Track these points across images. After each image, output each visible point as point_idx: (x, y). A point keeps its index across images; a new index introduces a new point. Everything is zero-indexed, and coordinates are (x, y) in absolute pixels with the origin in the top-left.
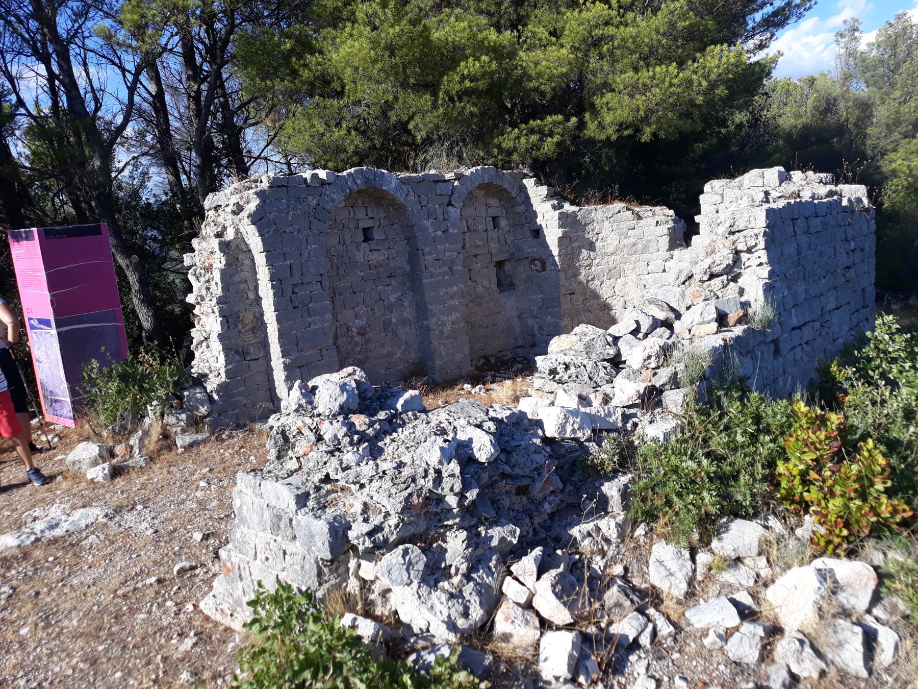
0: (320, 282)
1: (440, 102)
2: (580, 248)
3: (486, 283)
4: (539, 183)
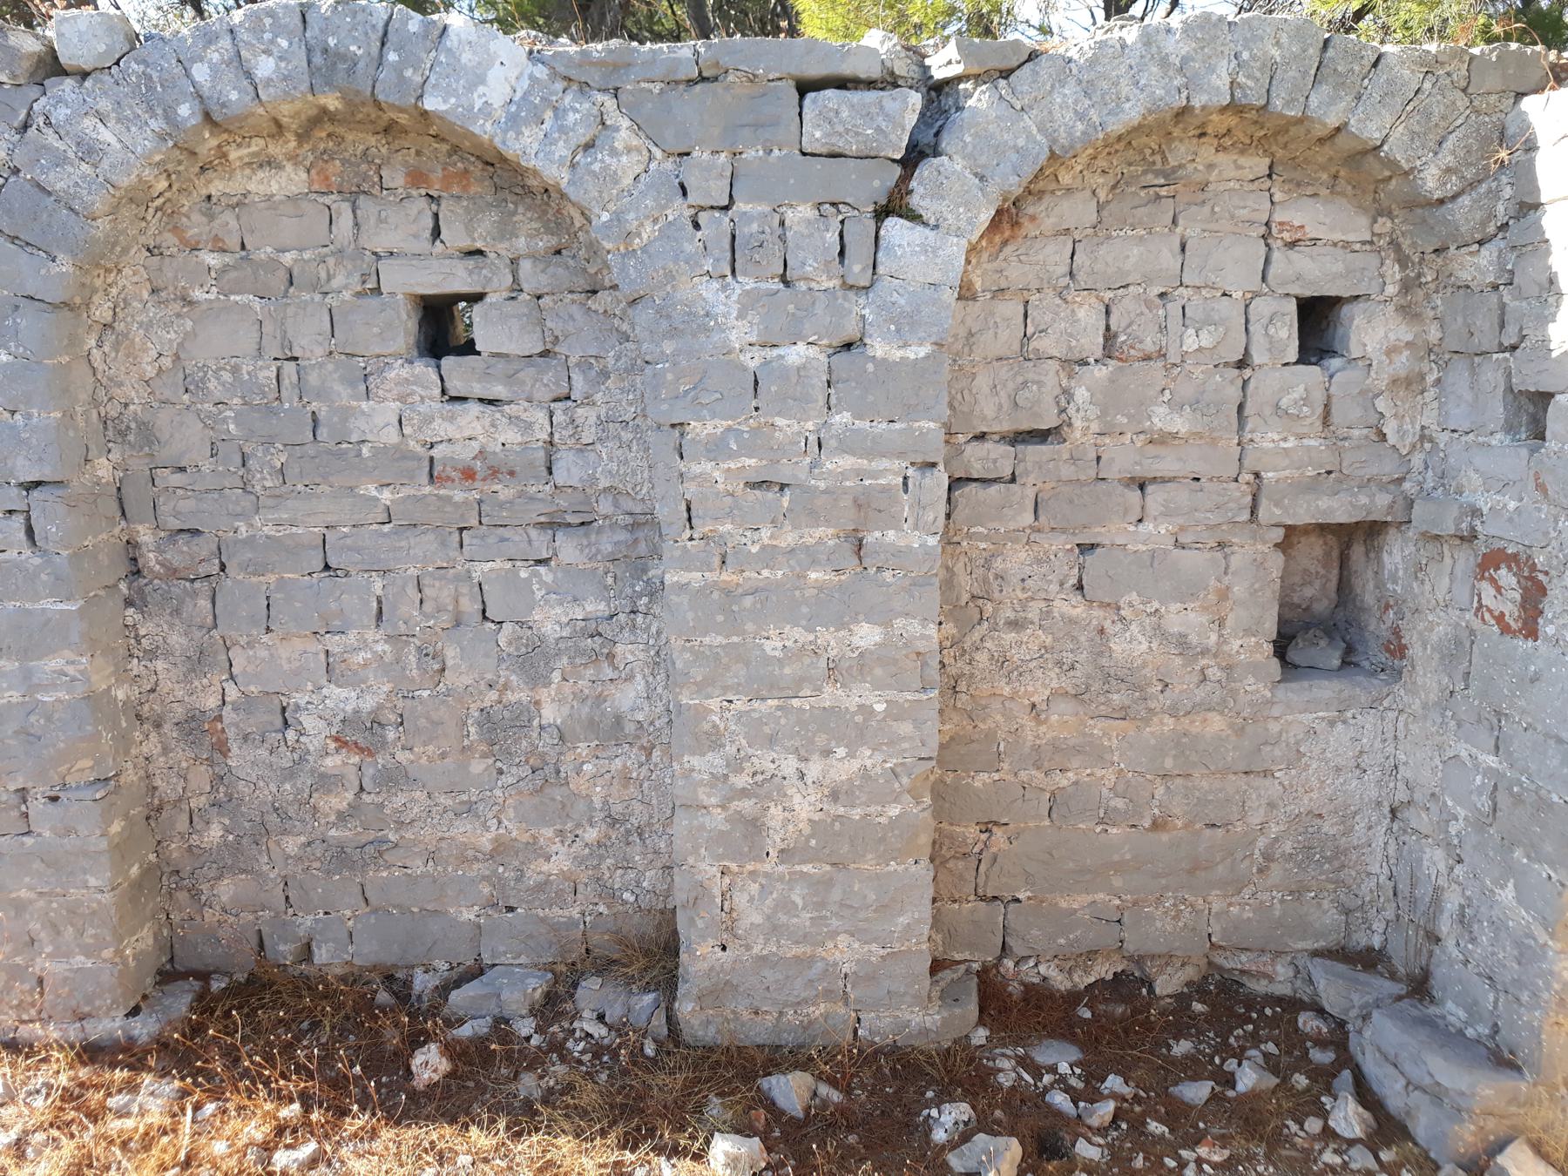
3: (1186, 619)
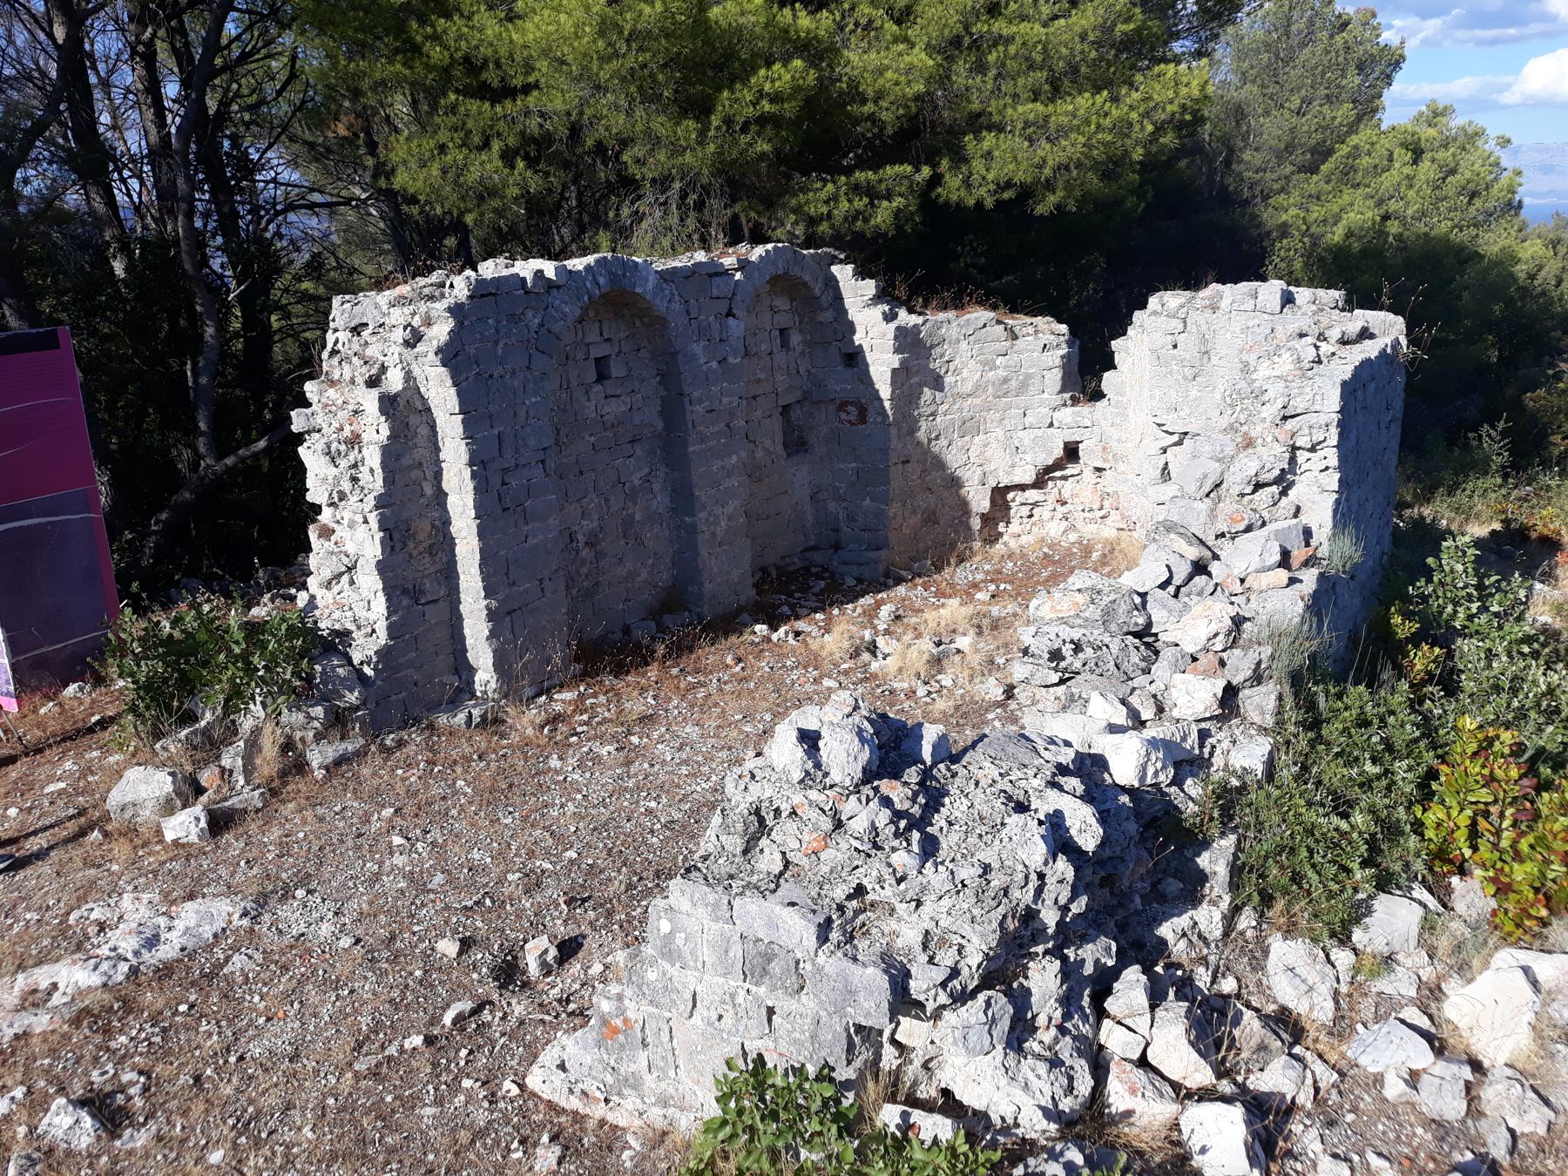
0: (543, 462)
1: (712, 133)
2: (921, 385)
3: (768, 443)
4: (861, 274)
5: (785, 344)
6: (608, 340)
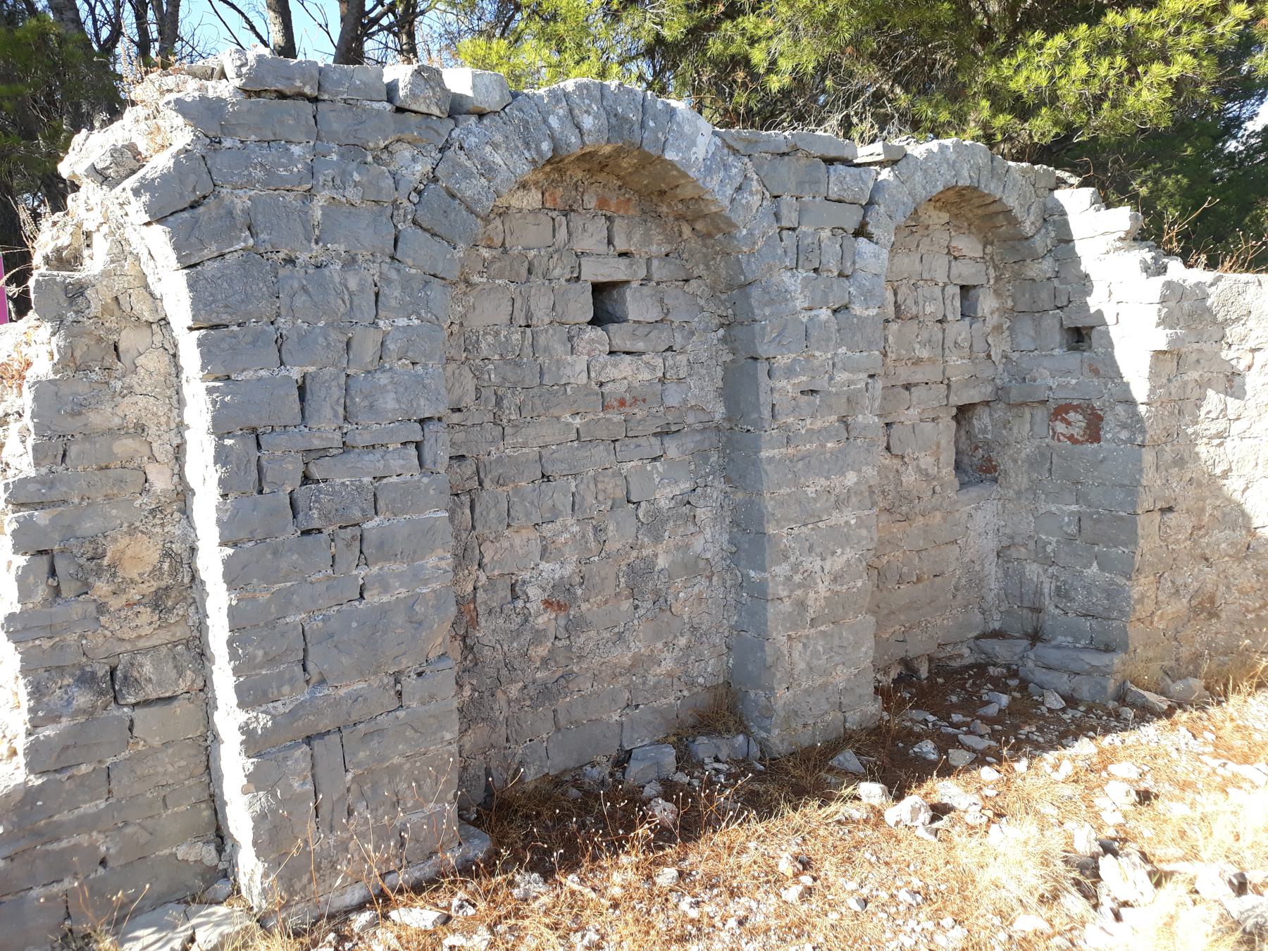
0: (418, 446)
2: (1203, 385)
3: (927, 461)
4: (1110, 191)
5: (968, 312)
6: (623, 255)
